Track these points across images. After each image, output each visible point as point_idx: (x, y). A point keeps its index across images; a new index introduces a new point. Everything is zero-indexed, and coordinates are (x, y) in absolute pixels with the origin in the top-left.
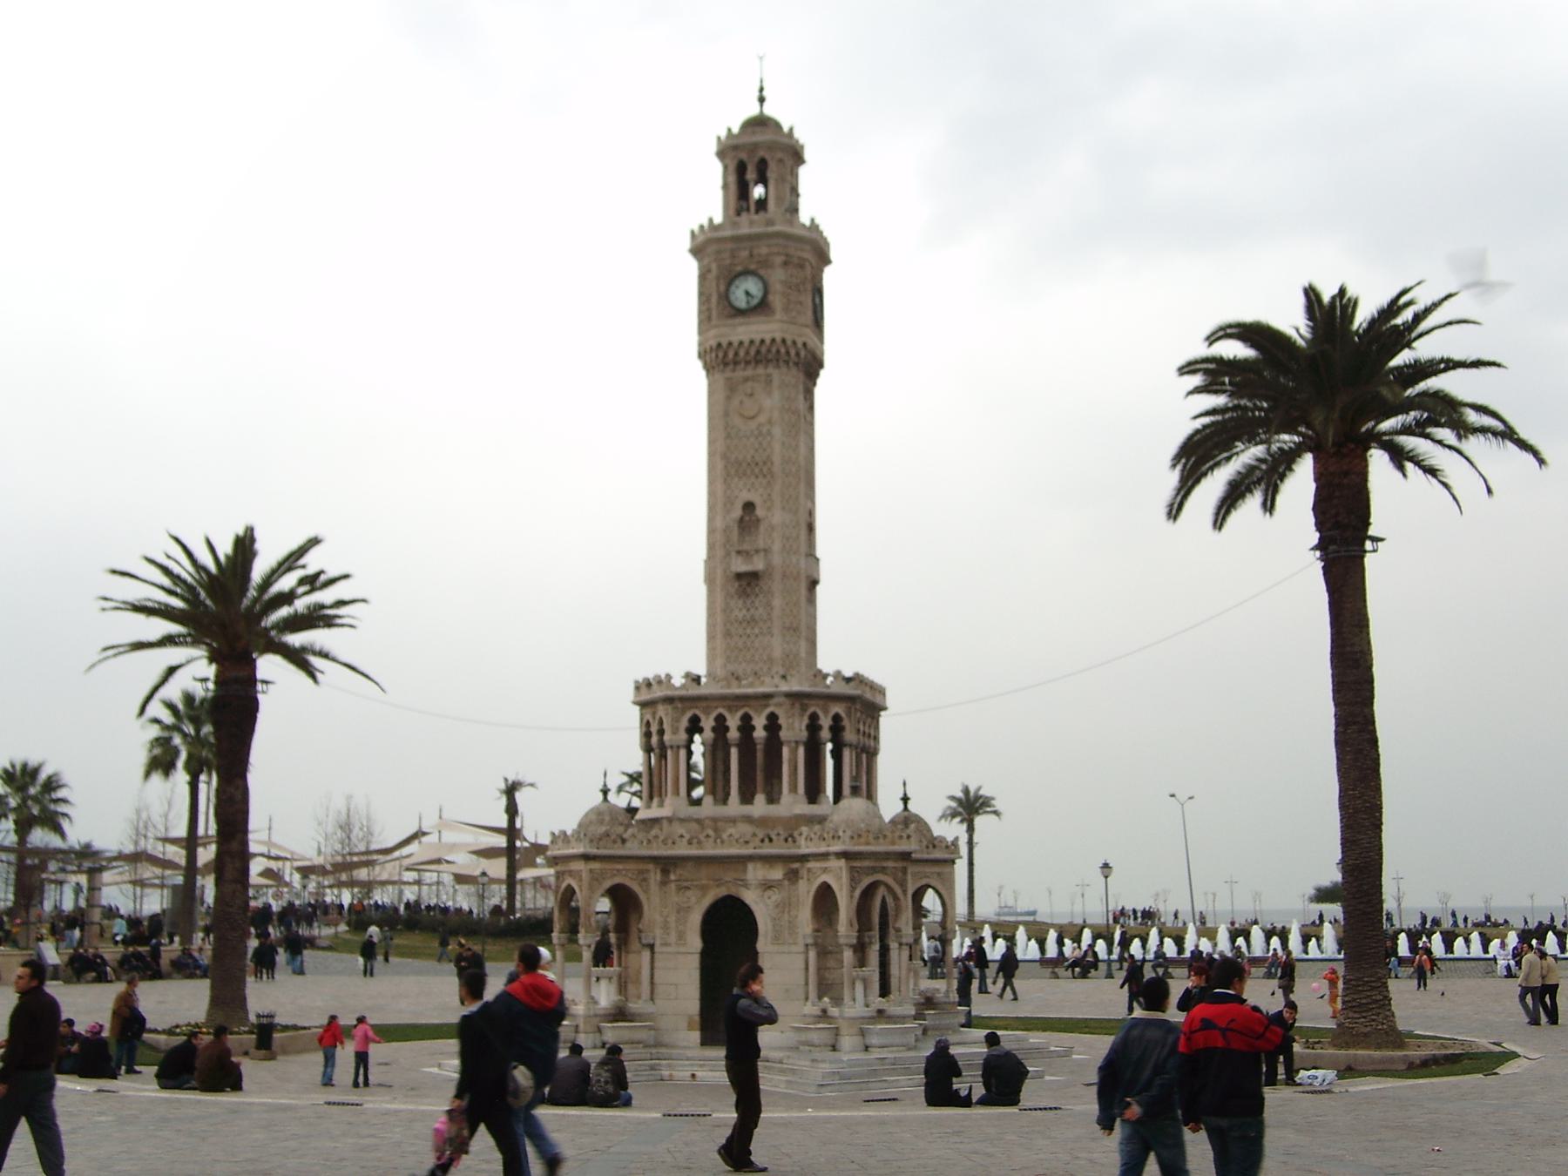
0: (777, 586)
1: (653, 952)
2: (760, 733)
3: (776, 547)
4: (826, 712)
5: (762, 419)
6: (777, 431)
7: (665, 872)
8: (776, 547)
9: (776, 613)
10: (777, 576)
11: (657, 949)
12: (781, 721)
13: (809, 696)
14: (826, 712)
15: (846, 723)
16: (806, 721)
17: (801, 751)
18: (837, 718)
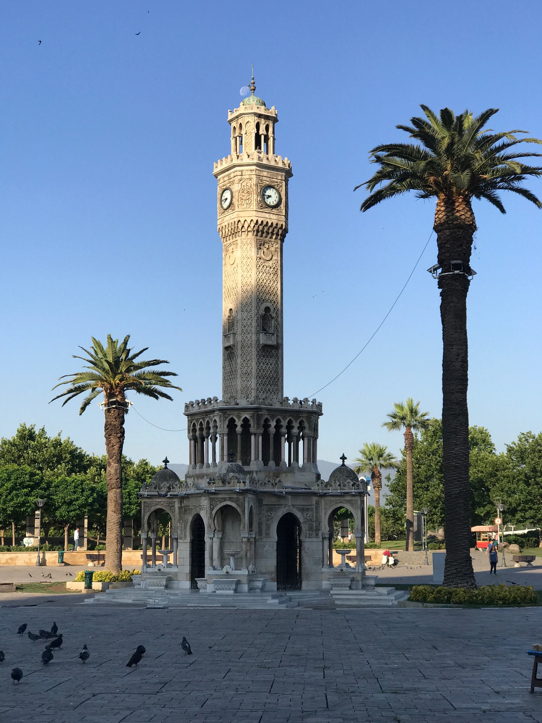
0: (239, 352)
1: (177, 542)
2: (272, 430)
3: (239, 331)
4: (239, 417)
5: (235, 265)
6: (240, 270)
7: (181, 502)
8: (239, 331)
9: (239, 366)
10: (239, 347)
11: (179, 541)
12: (218, 424)
13: (227, 409)
14: (239, 417)
15: (251, 423)
16: (227, 423)
17: (225, 438)
18: (246, 420)
